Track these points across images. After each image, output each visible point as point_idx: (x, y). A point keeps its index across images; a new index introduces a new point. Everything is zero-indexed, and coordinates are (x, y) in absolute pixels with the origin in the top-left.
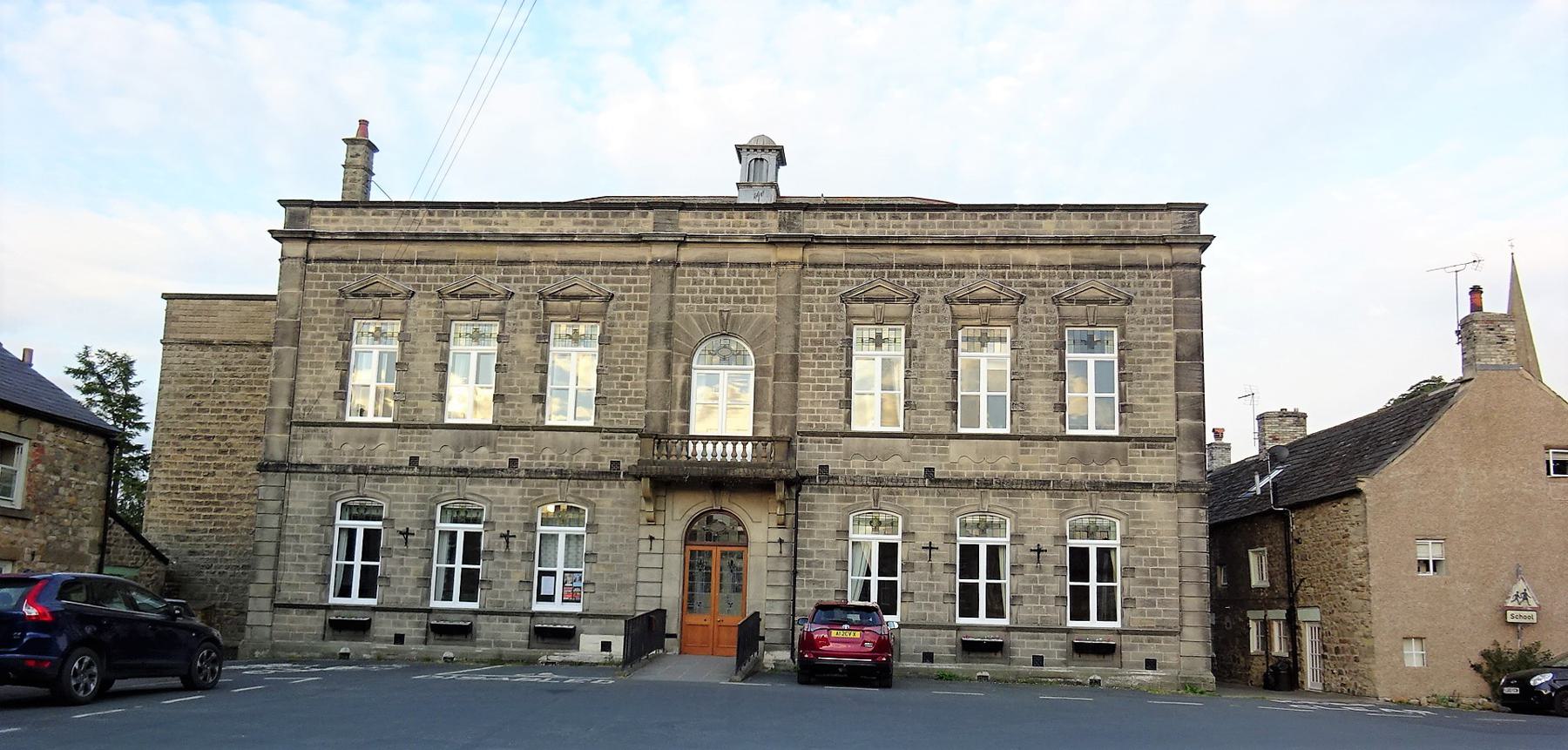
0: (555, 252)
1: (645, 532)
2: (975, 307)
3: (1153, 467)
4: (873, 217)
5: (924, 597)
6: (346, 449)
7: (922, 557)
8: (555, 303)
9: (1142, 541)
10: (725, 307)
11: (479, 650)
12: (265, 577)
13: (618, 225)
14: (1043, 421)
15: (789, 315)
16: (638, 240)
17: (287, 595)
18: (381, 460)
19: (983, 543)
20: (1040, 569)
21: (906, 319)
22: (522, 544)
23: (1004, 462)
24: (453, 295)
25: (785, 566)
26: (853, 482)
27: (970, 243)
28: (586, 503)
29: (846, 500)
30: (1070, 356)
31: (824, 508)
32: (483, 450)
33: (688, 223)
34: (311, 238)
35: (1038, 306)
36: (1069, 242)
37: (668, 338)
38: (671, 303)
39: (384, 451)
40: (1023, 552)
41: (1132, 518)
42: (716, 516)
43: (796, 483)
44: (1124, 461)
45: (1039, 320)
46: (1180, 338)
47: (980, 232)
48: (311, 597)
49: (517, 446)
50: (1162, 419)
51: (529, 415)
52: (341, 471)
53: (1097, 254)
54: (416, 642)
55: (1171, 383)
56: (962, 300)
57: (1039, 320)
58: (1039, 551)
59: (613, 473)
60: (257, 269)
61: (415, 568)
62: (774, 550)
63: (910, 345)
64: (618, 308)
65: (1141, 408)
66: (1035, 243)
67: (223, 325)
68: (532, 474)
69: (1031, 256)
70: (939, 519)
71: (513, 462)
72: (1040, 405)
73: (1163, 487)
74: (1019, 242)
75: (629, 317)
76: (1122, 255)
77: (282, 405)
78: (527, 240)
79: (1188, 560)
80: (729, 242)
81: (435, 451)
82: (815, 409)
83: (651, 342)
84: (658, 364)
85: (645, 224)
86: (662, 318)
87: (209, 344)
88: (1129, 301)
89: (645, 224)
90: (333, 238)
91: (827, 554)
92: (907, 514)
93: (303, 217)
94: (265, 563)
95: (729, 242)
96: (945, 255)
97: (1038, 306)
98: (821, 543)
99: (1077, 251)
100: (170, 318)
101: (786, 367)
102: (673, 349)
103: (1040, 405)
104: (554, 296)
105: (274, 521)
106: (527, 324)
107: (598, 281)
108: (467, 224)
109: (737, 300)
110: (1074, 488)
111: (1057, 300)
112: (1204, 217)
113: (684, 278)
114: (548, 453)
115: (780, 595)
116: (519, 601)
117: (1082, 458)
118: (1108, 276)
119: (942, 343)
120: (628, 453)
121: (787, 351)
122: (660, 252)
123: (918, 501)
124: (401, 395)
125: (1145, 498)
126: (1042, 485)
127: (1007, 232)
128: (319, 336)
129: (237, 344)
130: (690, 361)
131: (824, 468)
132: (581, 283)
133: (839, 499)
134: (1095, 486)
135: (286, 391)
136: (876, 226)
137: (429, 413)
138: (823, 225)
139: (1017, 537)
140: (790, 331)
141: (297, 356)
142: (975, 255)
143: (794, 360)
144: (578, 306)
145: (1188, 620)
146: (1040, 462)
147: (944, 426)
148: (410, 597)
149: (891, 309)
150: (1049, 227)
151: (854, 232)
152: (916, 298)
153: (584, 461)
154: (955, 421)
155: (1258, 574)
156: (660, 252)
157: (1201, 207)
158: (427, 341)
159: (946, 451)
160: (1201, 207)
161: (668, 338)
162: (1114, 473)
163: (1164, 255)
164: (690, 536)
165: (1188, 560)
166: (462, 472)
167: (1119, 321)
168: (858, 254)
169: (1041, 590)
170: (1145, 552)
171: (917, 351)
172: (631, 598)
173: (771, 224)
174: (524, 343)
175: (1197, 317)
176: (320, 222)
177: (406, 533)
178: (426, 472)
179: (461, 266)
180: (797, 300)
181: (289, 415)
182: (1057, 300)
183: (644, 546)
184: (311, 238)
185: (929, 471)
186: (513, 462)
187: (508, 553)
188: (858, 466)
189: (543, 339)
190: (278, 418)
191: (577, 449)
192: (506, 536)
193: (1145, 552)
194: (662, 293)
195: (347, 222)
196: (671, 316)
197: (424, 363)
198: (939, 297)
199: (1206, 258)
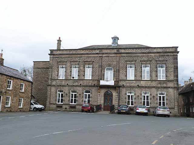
0: (86, 56)
1: (98, 94)
2: (144, 62)
3: (171, 85)
4: (130, 50)
5: (137, 103)
6: (59, 83)
7: (137, 97)
8: (85, 63)
9: (169, 95)
10: (109, 63)
11: (76, 110)
12: (48, 100)
13: (94, 52)
14: (154, 78)
15: (118, 63)
16: (97, 54)
17: (51, 102)
18: (63, 84)
19: (146, 95)
20: (154, 99)
21: (135, 64)
22: (82, 96)
23: (149, 84)
24: (72, 62)
25: (118, 99)
26: (128, 87)
27: (143, 53)
28: (91, 90)
29: (126, 89)
30: (158, 69)
31: (123, 91)
32: (76, 83)
33: (104, 51)
34: (54, 55)
35: (154, 62)
36: (158, 53)
37: (101, 67)
38: (102, 62)
39: (63, 83)
40: (151, 97)
41: (167, 92)
42: (108, 92)
43: (120, 87)
44: (166, 84)
45: (154, 64)
46: (174, 66)
47: (145, 51)
48: (54, 102)
49: (81, 82)
50: (172, 78)
51: (83, 78)
52: (58, 86)
53: (162, 54)
54: (68, 109)
55: (173, 72)
56: (143, 61)
57: (154, 64)
58: (154, 96)
59: (94, 86)
60: (47, 58)
61: (68, 99)
62: (116, 96)
63: (135, 68)
64: (94, 63)
65: (169, 76)
66: (153, 53)
67: (41, 66)
68: (83, 86)
69: (152, 55)
70: (139, 92)
71: (81, 84)
72: (154, 75)
73: (172, 88)
74: (151, 53)
75: (96, 64)
76: (166, 54)
77: (50, 77)
78: (82, 54)
79: (176, 98)
80: (110, 54)
81: (70, 83)
82: (122, 77)
83: (99, 68)
84: (100, 70)
85: (98, 52)
86: (100, 64)
87: (39, 68)
88: (167, 61)
89: (98, 52)
90: (56, 55)
91: (124, 97)
92: (135, 91)
93: (53, 52)
94: (48, 98)
95: (110, 54)
96: (140, 55)
97: (154, 62)
98: (123, 95)
99: (159, 54)
100: (34, 65)
101: (118, 71)
102: (102, 68)
103: (154, 75)
104: (86, 62)
105: (49, 93)
106: (82, 66)
107: (92, 59)
108: (74, 52)
109: (111, 62)
111: (156, 61)
112: (178, 49)
113: (104, 59)
114: (85, 83)
115: (117, 103)
116: (82, 103)
117: (160, 83)
118: (164, 57)
119: (140, 67)
120: (96, 83)
121: (118, 69)
122: (100, 55)
123: (136, 89)
124: (66, 76)
125: (169, 89)
126: (154, 87)
127: (149, 51)
128: (55, 68)
129: (43, 68)
130: (104, 70)
131: (123, 85)
132: (89, 60)
133: (126, 89)
134: (162, 87)
135: (51, 75)
136: (130, 51)
137: (69, 78)
138: (123, 51)
139: (151, 95)
140: (118, 66)
141: (52, 70)
142: (145, 55)
143: (119, 70)
144: (89, 63)
145: (176, 107)
146: (154, 84)
147: (140, 79)
148: (67, 103)
149: (132, 63)
150: (155, 51)
151: (127, 52)
152: (136, 61)
153: (90, 84)
154: (142, 78)
156: (100, 55)
157: (178, 47)
158: (69, 68)
159: (140, 82)
160: (178, 47)
161: (101, 67)
162: (165, 85)
163: (172, 54)
164: (105, 94)
165: (176, 98)
166: (74, 86)
167: (165, 64)
168: (128, 55)
169: (154, 102)
170: (169, 97)
171: (136, 68)
172: (97, 103)
173: (115, 51)
174: (82, 68)
176: (55, 53)
177: (67, 94)
178: (69, 86)
179: (73, 58)
180: (119, 61)
181: (51, 78)
182: (156, 61)
183: (98, 96)
184: (54, 55)
185: (138, 85)
186: (81, 84)
187: (80, 97)
188: (128, 85)
189: (84, 68)
190: (50, 79)
191: (89, 83)
192: (80, 94)
193: (169, 97)
194: (100, 61)
195: (58, 52)
196: (102, 64)
197: (69, 71)
198: (139, 60)
199: (178, 55)
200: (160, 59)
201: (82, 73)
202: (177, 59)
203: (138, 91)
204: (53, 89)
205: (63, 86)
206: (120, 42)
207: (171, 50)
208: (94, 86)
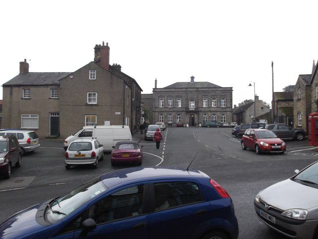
3: (228, 110)
6: (160, 110)
13: (182, 90)
23: (216, 110)
31: (201, 113)
39: (163, 110)
49: (175, 109)
50: (229, 106)
51: (175, 106)
59: (183, 111)
81: (168, 110)
82: (200, 105)
89: (184, 90)
110: (221, 111)
120: (184, 109)
132: (180, 94)
136: (205, 90)
146: (219, 109)
150: (220, 89)
155: (240, 118)
173: (195, 90)
175: (232, 97)
200: (223, 94)
201: (175, 103)
202: (232, 94)
203: (210, 114)
204: (157, 114)
205: (163, 112)
206: (195, 80)
207: (229, 89)
208: (183, 111)
